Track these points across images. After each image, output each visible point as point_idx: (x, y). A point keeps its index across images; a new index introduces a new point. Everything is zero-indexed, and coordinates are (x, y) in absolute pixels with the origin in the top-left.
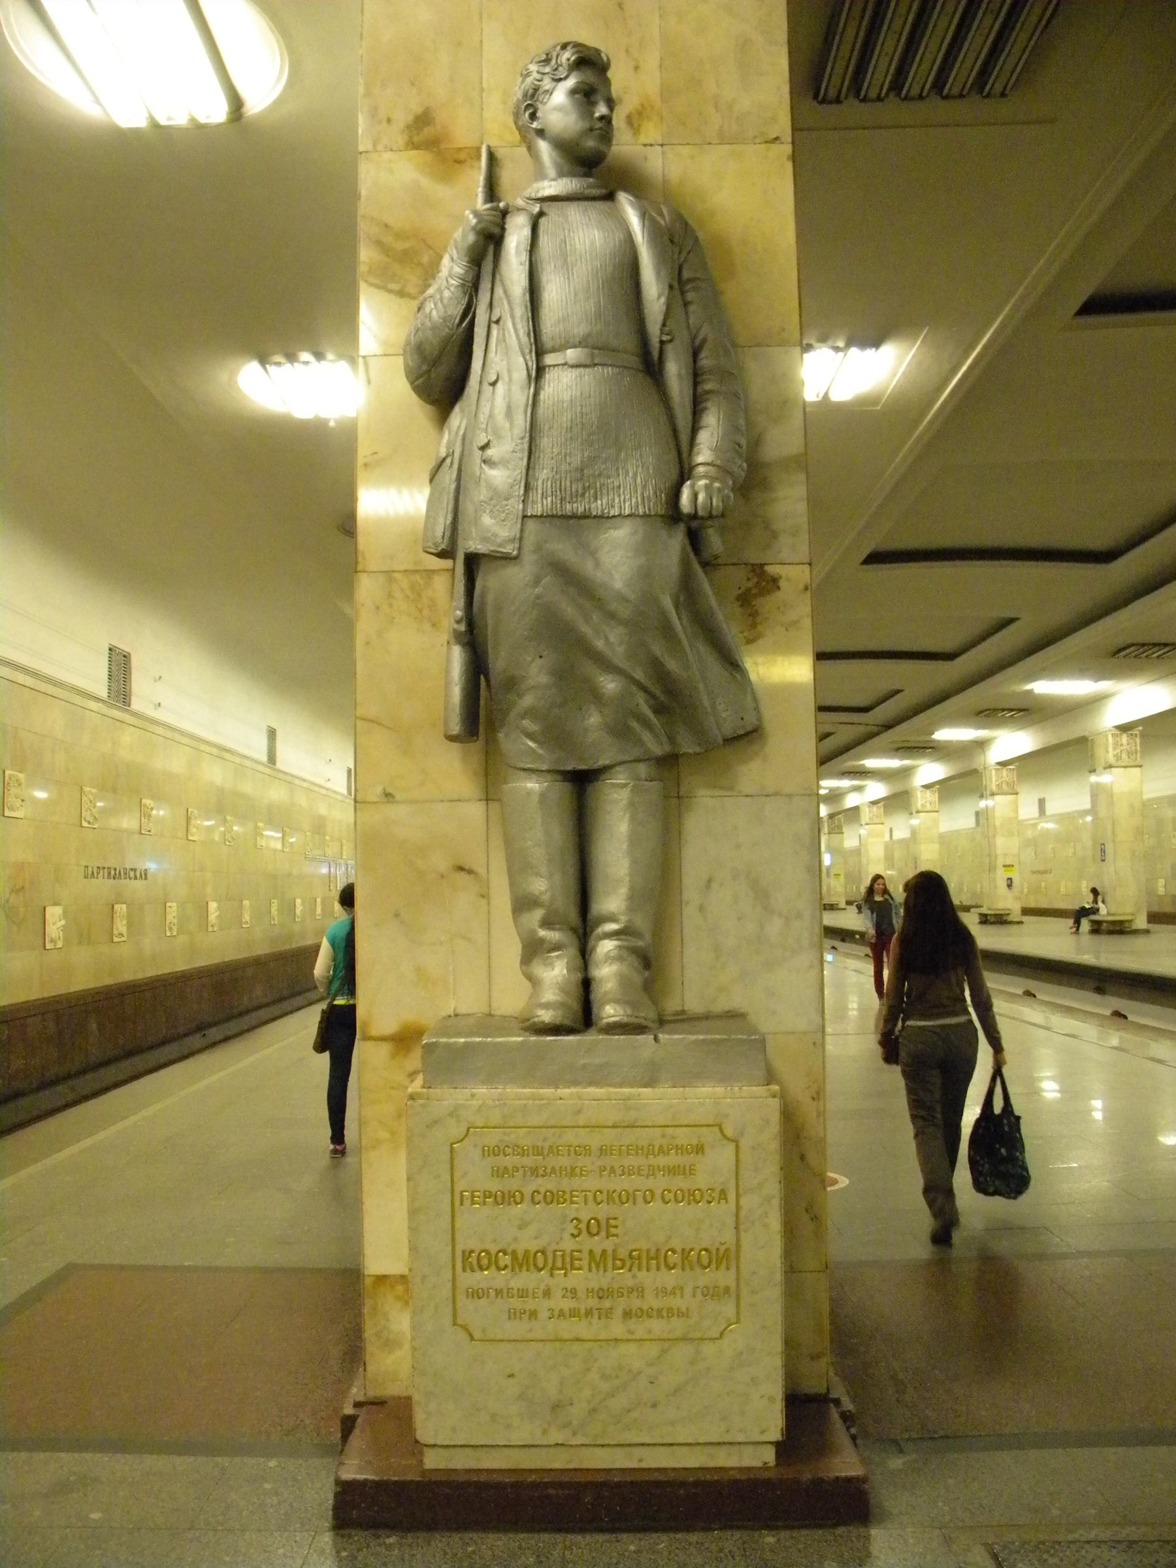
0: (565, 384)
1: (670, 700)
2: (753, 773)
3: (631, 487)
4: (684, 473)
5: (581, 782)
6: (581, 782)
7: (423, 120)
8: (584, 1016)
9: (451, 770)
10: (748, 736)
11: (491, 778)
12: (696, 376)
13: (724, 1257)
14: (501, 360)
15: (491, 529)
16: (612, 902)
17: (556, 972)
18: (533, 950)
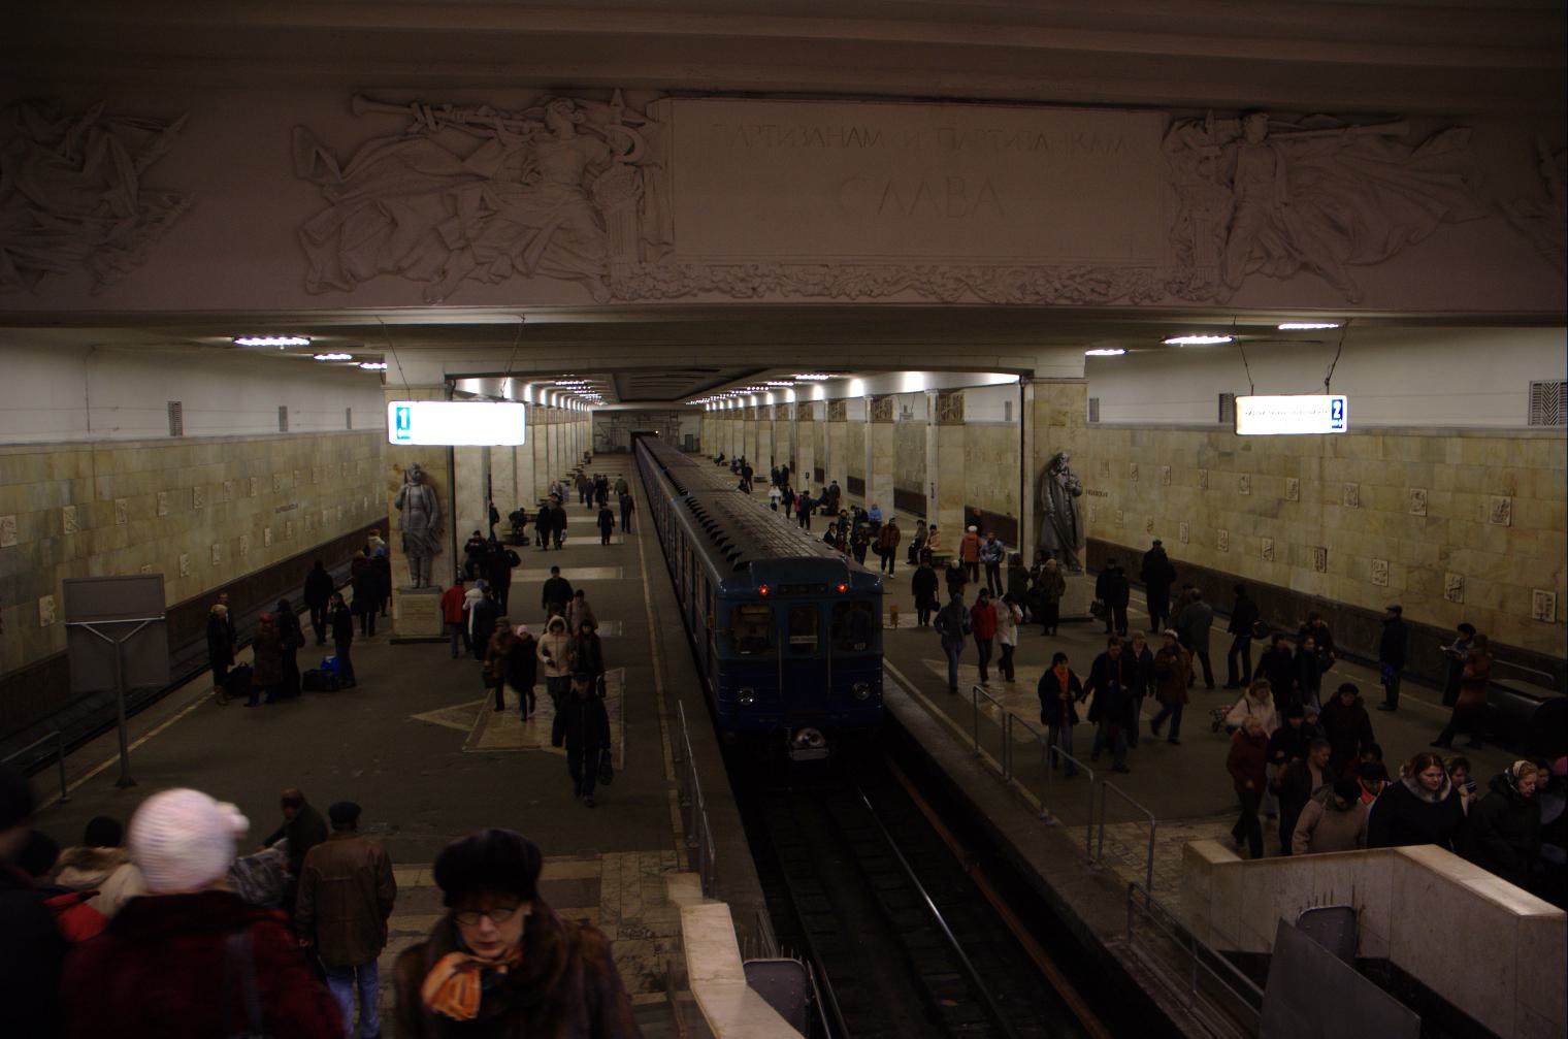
0: (414, 512)
1: (429, 549)
2: (441, 556)
3: (422, 525)
4: (429, 522)
5: (418, 560)
6: (418, 560)
7: (396, 465)
8: (417, 587)
9: (403, 556)
10: (441, 551)
11: (408, 557)
12: (431, 508)
13: (433, 614)
14: (406, 508)
15: (405, 530)
16: (422, 573)
17: (415, 581)
18: (413, 579)
